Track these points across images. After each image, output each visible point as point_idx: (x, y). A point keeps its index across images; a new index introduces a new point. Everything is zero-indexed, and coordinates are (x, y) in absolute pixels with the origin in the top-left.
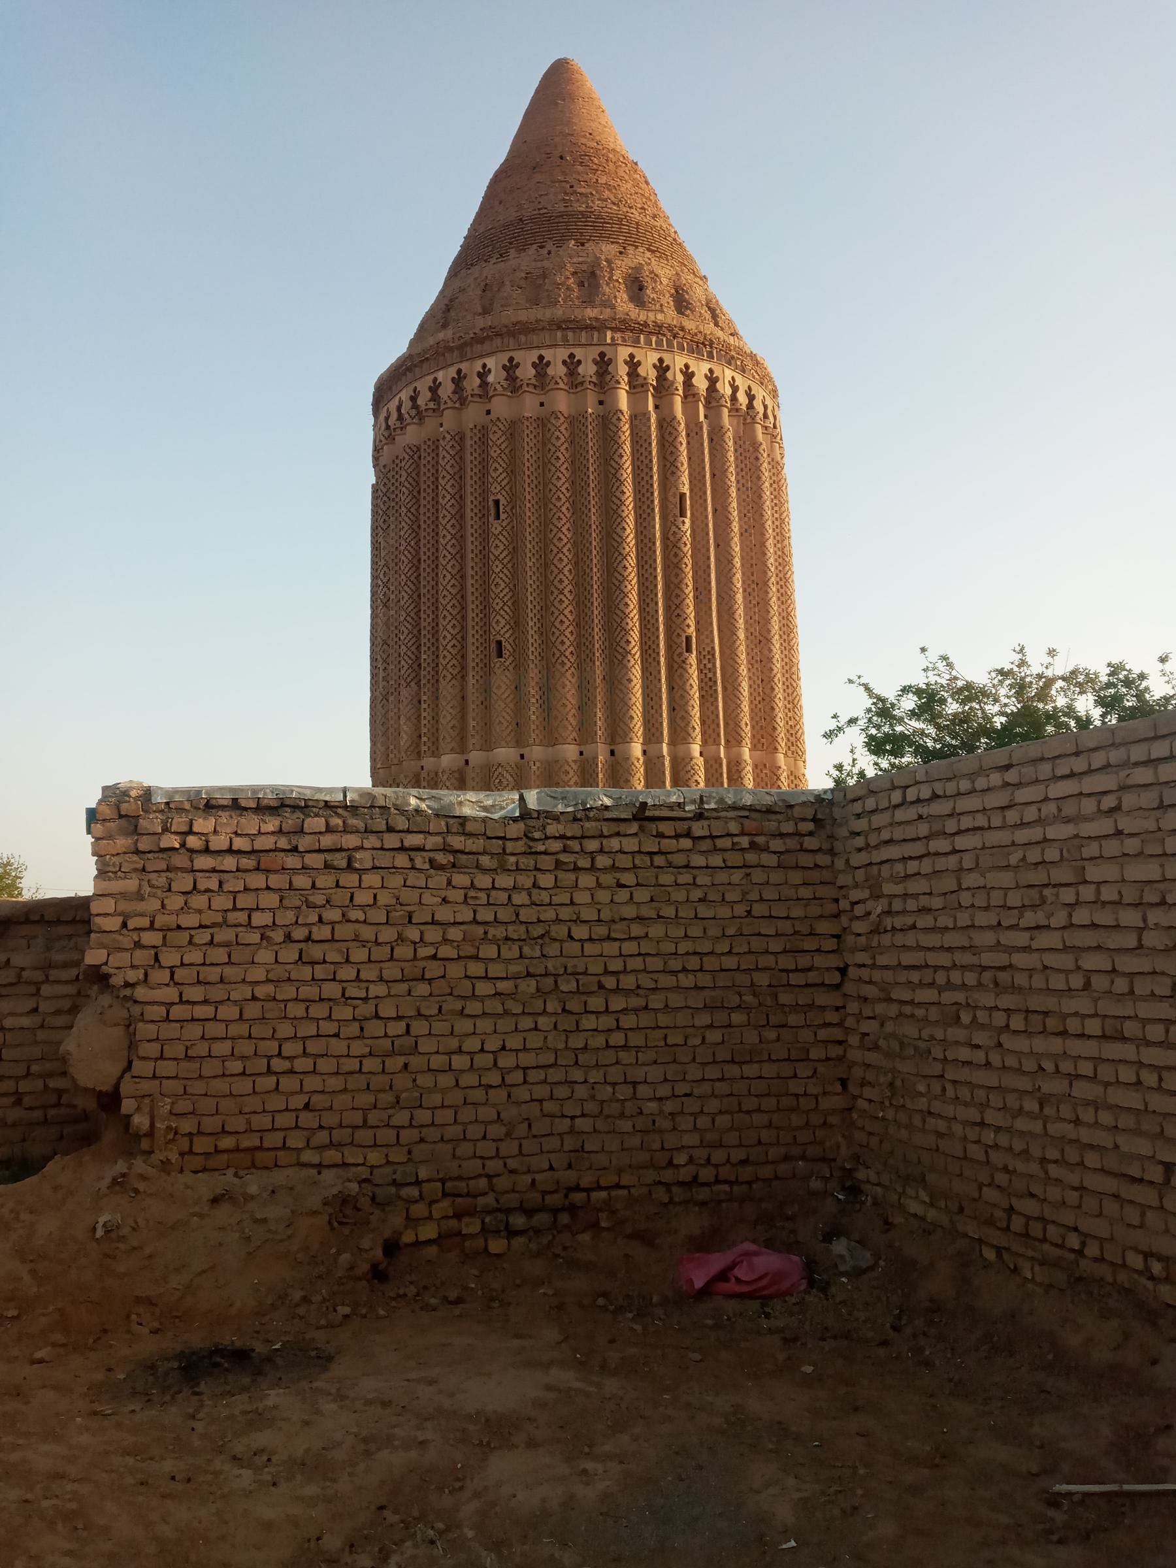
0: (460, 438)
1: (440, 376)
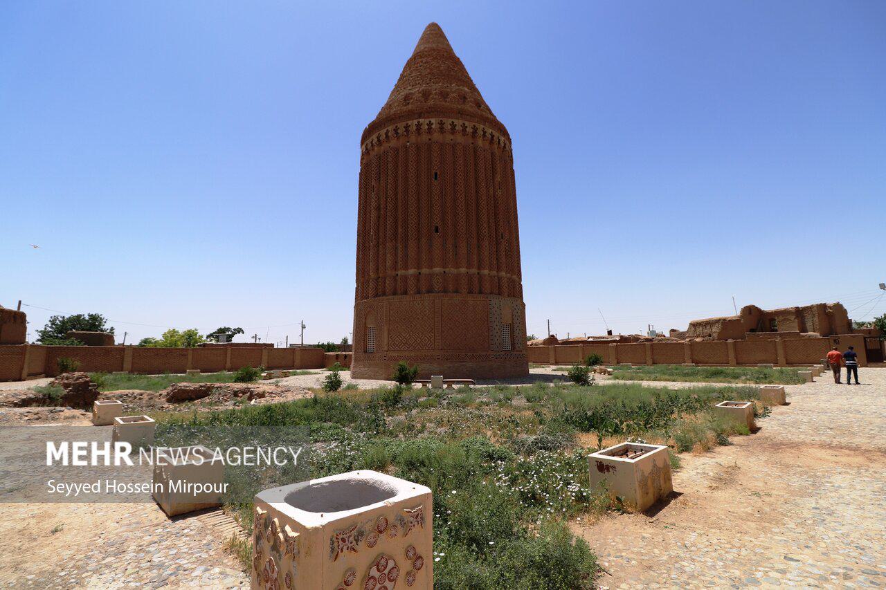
0: (418, 148)
1: (410, 123)
